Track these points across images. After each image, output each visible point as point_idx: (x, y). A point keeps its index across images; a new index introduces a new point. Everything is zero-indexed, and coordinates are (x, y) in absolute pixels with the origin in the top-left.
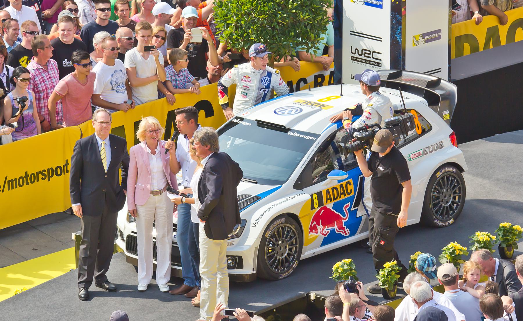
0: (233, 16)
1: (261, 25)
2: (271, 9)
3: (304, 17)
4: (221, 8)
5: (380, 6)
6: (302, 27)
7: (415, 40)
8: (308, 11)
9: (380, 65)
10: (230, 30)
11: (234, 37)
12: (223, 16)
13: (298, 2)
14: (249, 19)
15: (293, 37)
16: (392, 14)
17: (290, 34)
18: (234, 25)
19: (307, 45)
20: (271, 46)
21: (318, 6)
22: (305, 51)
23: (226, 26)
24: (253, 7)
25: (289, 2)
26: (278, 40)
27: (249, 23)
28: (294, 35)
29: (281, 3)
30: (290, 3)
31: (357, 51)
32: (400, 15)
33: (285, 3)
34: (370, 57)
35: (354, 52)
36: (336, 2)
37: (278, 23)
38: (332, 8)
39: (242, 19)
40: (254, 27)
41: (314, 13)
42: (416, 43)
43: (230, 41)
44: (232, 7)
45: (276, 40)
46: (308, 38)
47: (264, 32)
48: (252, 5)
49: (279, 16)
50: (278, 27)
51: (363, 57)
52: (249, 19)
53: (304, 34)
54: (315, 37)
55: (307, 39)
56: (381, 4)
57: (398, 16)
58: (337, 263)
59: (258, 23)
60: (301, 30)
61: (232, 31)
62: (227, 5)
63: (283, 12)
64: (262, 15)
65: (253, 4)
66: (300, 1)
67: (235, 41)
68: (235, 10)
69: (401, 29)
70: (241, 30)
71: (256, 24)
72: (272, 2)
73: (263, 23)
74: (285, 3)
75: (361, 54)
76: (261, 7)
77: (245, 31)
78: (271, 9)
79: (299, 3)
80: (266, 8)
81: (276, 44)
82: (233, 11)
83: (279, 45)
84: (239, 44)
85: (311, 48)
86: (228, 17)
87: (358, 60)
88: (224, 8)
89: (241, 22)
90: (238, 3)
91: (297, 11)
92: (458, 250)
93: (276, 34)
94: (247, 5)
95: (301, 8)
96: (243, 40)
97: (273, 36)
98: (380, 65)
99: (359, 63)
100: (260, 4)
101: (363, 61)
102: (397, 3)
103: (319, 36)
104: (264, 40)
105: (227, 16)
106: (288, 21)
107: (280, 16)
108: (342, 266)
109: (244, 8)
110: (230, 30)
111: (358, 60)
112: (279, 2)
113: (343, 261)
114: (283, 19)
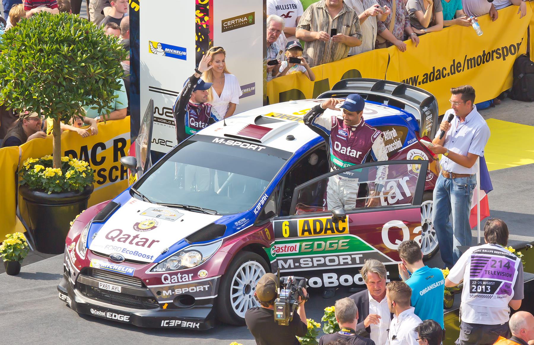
0: (12, 72)
1: (44, 81)
3: (95, 71)
5: (184, 58)
6: (93, 84)
8: (100, 64)
11: (14, 96)
13: (88, 54)
14: (30, 75)
15: (83, 95)
17: (80, 91)
18: (13, 82)
19: (99, 104)
20: (57, 106)
21: (111, 58)
22: (96, 111)
23: (3, 83)
24: (35, 60)
25: (77, 54)
26: (66, 100)
27: (30, 79)
29: (68, 55)
33: (72, 55)
34: (172, 117)
36: (131, 53)
37: (65, 79)
38: (128, 60)
39: (22, 75)
40: (36, 83)
41: (106, 67)
43: (9, 101)
44: (11, 61)
45: (63, 98)
47: (49, 90)
48: (34, 57)
49: (66, 71)
50: (64, 83)
51: (164, 117)
52: (30, 75)
53: (95, 91)
54: (108, 94)
56: (185, 54)
59: (41, 79)
60: (92, 86)
62: (5, 59)
63: (71, 65)
64: (46, 70)
65: (36, 57)
66: (90, 53)
67: (15, 101)
70: (22, 87)
71: (39, 80)
72: (57, 54)
73: (47, 78)
74: (72, 55)
75: (162, 113)
76: (44, 60)
79: (89, 54)
80: (51, 61)
82: (12, 66)
83: (66, 104)
84: (19, 104)
85: (103, 107)
86: (6, 73)
87: (159, 120)
90: (18, 56)
91: (87, 65)
93: (62, 92)
94: (28, 58)
96: (22, 100)
97: (60, 94)
99: (160, 123)
100: (43, 56)
101: (165, 121)
103: (112, 93)
105: (5, 71)
106: (76, 76)
107: (67, 70)
109: (25, 62)
111: (159, 120)
114: (70, 73)
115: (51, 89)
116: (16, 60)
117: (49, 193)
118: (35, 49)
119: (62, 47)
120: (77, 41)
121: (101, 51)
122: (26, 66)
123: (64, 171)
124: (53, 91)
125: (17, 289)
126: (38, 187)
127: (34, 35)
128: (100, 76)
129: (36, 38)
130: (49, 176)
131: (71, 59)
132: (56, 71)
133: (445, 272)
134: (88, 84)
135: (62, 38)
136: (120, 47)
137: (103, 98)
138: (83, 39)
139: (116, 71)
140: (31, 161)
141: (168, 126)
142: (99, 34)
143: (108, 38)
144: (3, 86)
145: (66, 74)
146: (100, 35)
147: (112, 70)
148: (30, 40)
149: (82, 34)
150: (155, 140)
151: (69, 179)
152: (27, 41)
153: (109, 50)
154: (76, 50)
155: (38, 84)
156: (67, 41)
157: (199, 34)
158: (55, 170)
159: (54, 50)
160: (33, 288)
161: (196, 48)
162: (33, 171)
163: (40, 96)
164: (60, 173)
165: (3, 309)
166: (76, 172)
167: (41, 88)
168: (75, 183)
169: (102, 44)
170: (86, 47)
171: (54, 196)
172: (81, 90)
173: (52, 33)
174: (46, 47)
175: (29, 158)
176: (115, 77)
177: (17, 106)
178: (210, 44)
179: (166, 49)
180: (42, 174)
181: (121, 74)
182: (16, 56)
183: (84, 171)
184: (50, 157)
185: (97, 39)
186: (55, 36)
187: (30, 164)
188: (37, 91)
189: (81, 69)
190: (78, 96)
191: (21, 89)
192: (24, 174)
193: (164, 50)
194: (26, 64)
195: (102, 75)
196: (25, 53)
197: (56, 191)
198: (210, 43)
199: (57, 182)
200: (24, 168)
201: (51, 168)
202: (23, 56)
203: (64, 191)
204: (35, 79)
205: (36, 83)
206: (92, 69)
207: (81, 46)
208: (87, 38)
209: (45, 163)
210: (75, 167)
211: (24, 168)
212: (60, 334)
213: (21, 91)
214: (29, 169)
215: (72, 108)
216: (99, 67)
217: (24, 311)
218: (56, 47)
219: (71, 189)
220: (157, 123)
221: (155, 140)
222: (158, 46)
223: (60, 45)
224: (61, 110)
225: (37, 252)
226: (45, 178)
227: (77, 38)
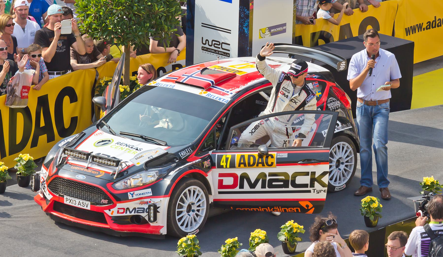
2: (128, 2)
3: (159, 9)
6: (157, 19)
9: (229, 55)
10: (89, 20)
11: (94, 26)
12: (84, 7)
14: (107, 11)
15: (149, 28)
16: (240, 8)
17: (146, 24)
23: (86, 16)
27: (107, 14)
31: (207, 42)
32: (248, 9)
34: (219, 48)
35: (204, 42)
37: (135, 15)
39: (101, 10)
40: (111, 17)
41: (168, 6)
42: (262, 35)
43: (90, 31)
45: (133, 29)
46: (163, 29)
47: (121, 23)
49: (135, 8)
51: (213, 47)
52: (107, 11)
54: (168, 29)
55: (161, 30)
57: (246, 10)
58: (182, 239)
60: (156, 21)
61: (92, 20)
64: (120, 7)
68: (95, 1)
69: (248, 22)
71: (114, 15)
75: (211, 44)
77: (104, 21)
78: (128, 2)
81: (131, 34)
82: (92, 2)
83: (135, 35)
84: (98, 33)
86: (88, 8)
91: (153, 4)
92: (296, 228)
96: (100, 30)
98: (229, 55)
99: (209, 53)
101: (213, 51)
104: (120, 30)
106: (143, 13)
108: (186, 242)
110: (89, 20)
113: (187, 237)
114: (139, 11)
122: (104, 3)
123: (131, 89)
124: (124, 24)
128: (163, 14)
133: (431, 179)
139: (175, 11)
140: (106, 79)
141: (216, 55)
145: (136, 11)
147: (173, 8)
155: (113, 18)
158: (124, 86)
163: (114, 28)
164: (128, 89)
167: (115, 21)
175: (104, 77)
176: (175, 13)
177: (96, 35)
181: (180, 13)
188: (112, 24)
189: (148, 7)
190: (144, 29)
192: (100, 89)
194: (104, 1)
195: (164, 13)
200: (100, 84)
201: (121, 85)
204: (111, 14)
206: (156, 8)
211: (100, 84)
213: (99, 23)
215: (139, 37)
216: (162, 6)
220: (207, 52)
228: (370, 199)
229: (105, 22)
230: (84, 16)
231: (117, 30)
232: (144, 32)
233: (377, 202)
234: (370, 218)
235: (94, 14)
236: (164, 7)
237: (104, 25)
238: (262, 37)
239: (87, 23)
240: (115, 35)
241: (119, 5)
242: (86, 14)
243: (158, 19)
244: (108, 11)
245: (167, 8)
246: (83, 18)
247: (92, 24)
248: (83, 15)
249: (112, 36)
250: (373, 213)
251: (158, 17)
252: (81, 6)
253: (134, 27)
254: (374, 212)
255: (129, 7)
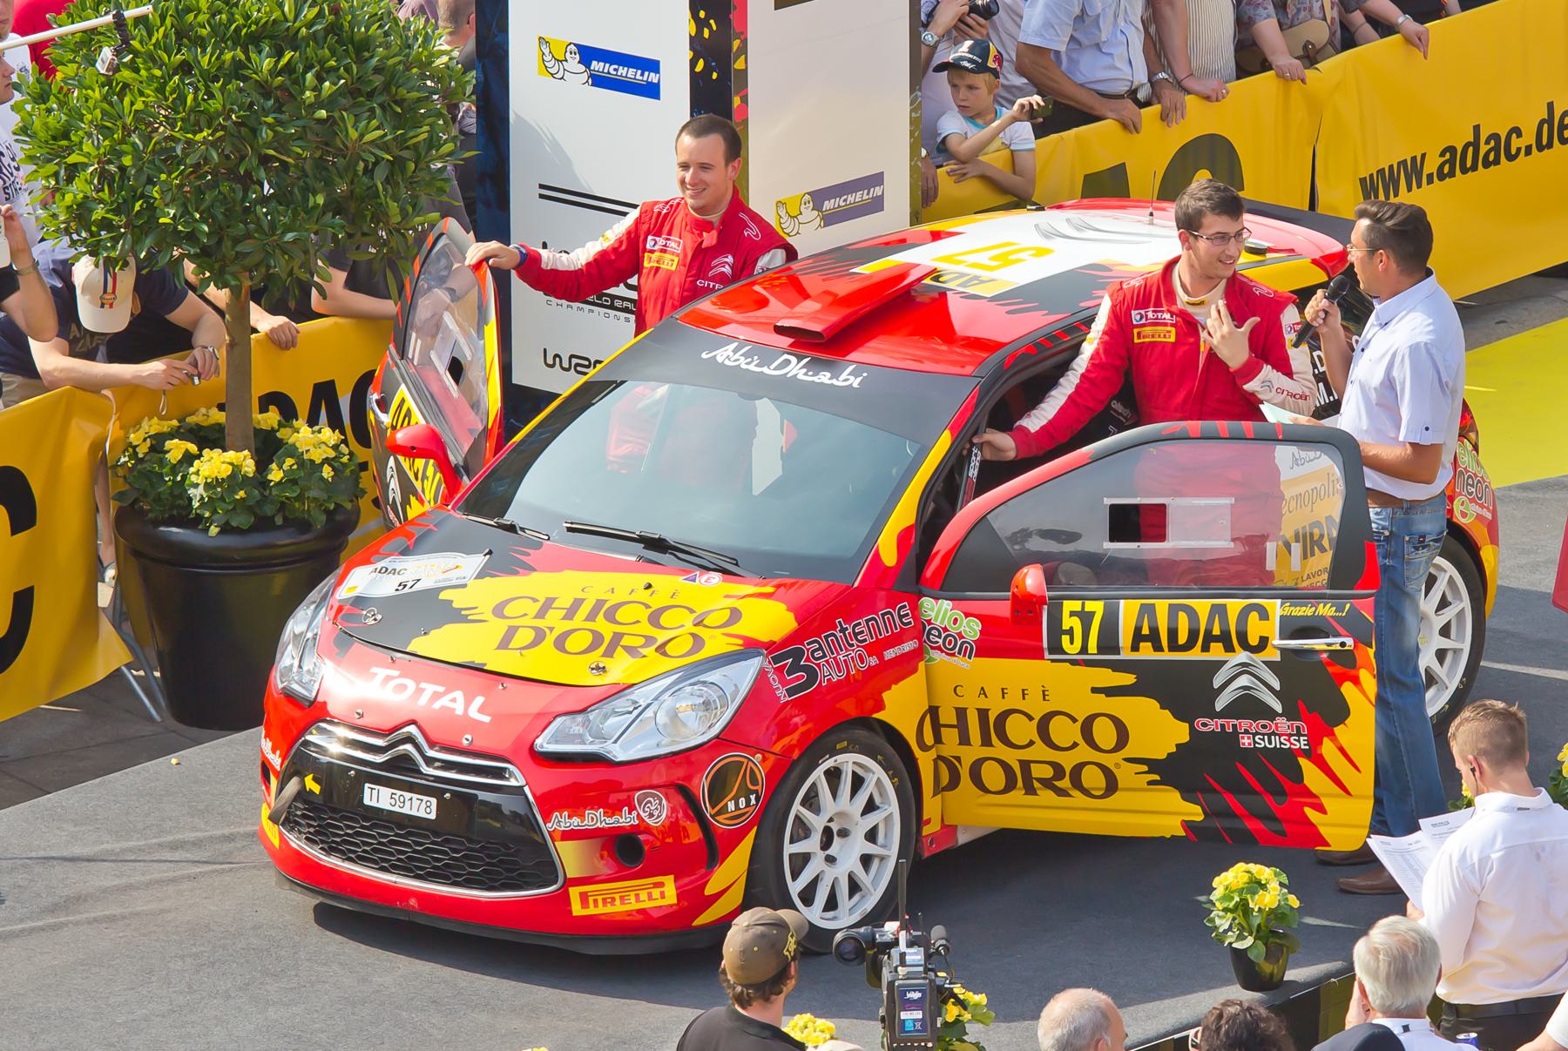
1: (197, 166)
4: (43, 106)
5: (652, 91)
6: (356, 174)
7: (785, 218)
8: (378, 111)
10: (79, 188)
11: (99, 213)
13: (339, 80)
15: (324, 213)
18: (96, 169)
20: (239, 248)
21: (415, 95)
23: (62, 172)
25: (304, 79)
26: (266, 229)
27: (149, 162)
28: (324, 205)
30: (307, 83)
36: (483, 79)
37: (265, 160)
39: (124, 147)
40: (169, 174)
44: (87, 101)
45: (258, 218)
46: (380, 216)
48: (161, 90)
49: (266, 134)
54: (404, 214)
56: (655, 81)
60: (352, 182)
61: (89, 190)
62: (66, 95)
63: (284, 117)
65: (168, 88)
66: (346, 75)
68: (98, 111)
70: (121, 188)
71: (179, 164)
72: (237, 80)
76: (195, 99)
79: (342, 81)
81: (255, 238)
84: (115, 240)
86: (70, 140)
88: (55, 106)
89: (119, 158)
90: (111, 87)
91: (336, 115)
94: (142, 94)
95: (351, 101)
102: (715, 76)
106: (299, 151)
107: (271, 134)
109: (132, 104)
110: (79, 188)
112: (266, 81)
114: (281, 143)
115: (220, 192)
116: (105, 98)
117: (214, 530)
118: (163, 64)
119: (253, 56)
120: (303, 38)
121: (383, 69)
125: (102, 843)
126: (175, 512)
127: (163, 18)
128: (379, 153)
129: (169, 27)
130: (214, 476)
131: (282, 94)
132: (232, 135)
134: (341, 178)
135: (253, 27)
136: (445, 59)
137: (387, 223)
138: (325, 29)
139: (430, 139)
140: (153, 426)
141: (602, 315)
142: (376, 14)
143: (407, 28)
144: (61, 183)
145: (268, 145)
146: (381, 19)
148: (150, 35)
149: (320, 14)
150: (557, 359)
151: (279, 483)
152: (138, 38)
153: (408, 69)
154: (301, 68)
155: (176, 178)
156: (271, 37)
157: (702, 14)
158: (231, 455)
159: (226, 65)
160: (154, 841)
161: (691, 61)
162: (162, 462)
164: (249, 467)
165: (54, 909)
166: (301, 462)
168: (300, 498)
169: (387, 46)
170: (333, 56)
171: (231, 541)
172: (314, 197)
173: (220, 13)
174: (204, 61)
176: (427, 153)
177: (106, 249)
178: (735, 48)
179: (594, 63)
180: (192, 470)
182: (103, 86)
183: (327, 461)
184: (219, 417)
185: (370, 33)
186: (231, 20)
187: (149, 437)
188: (173, 200)
189: (317, 128)
191: (119, 193)
193: (588, 66)
194: (136, 111)
195: (386, 149)
196: (134, 75)
197: (234, 524)
198: (736, 44)
199: (238, 497)
201: (220, 451)
202: (126, 86)
203: (263, 524)
204: (165, 161)
205: (169, 174)
207: (317, 56)
208: (334, 29)
209: (202, 433)
210: (297, 445)
212: (240, 989)
214: (146, 454)
217: (124, 917)
218: (233, 58)
219: (285, 519)
221: (557, 359)
222: (568, 54)
223: (246, 52)
224: (249, 261)
225: (173, 723)
226: (200, 480)
227: (304, 30)
228: (1247, 875)
229: (142, 196)
230: (56, 175)
231: (196, 225)
232: (307, 230)
233: (1274, 886)
234: (1251, 956)
235: (96, 166)
236: (385, 126)
237: (141, 206)
238: (788, 234)
239: (70, 204)
240: (184, 246)
241: (197, 123)
242: (65, 163)
243: (361, 173)
244: (153, 150)
245: (396, 128)
246: (53, 183)
247: (93, 205)
248: (51, 168)
249: (175, 253)
250: (1262, 934)
251: (362, 165)
252: (42, 135)
253: (264, 210)
254: (1267, 927)
255: (239, 132)
